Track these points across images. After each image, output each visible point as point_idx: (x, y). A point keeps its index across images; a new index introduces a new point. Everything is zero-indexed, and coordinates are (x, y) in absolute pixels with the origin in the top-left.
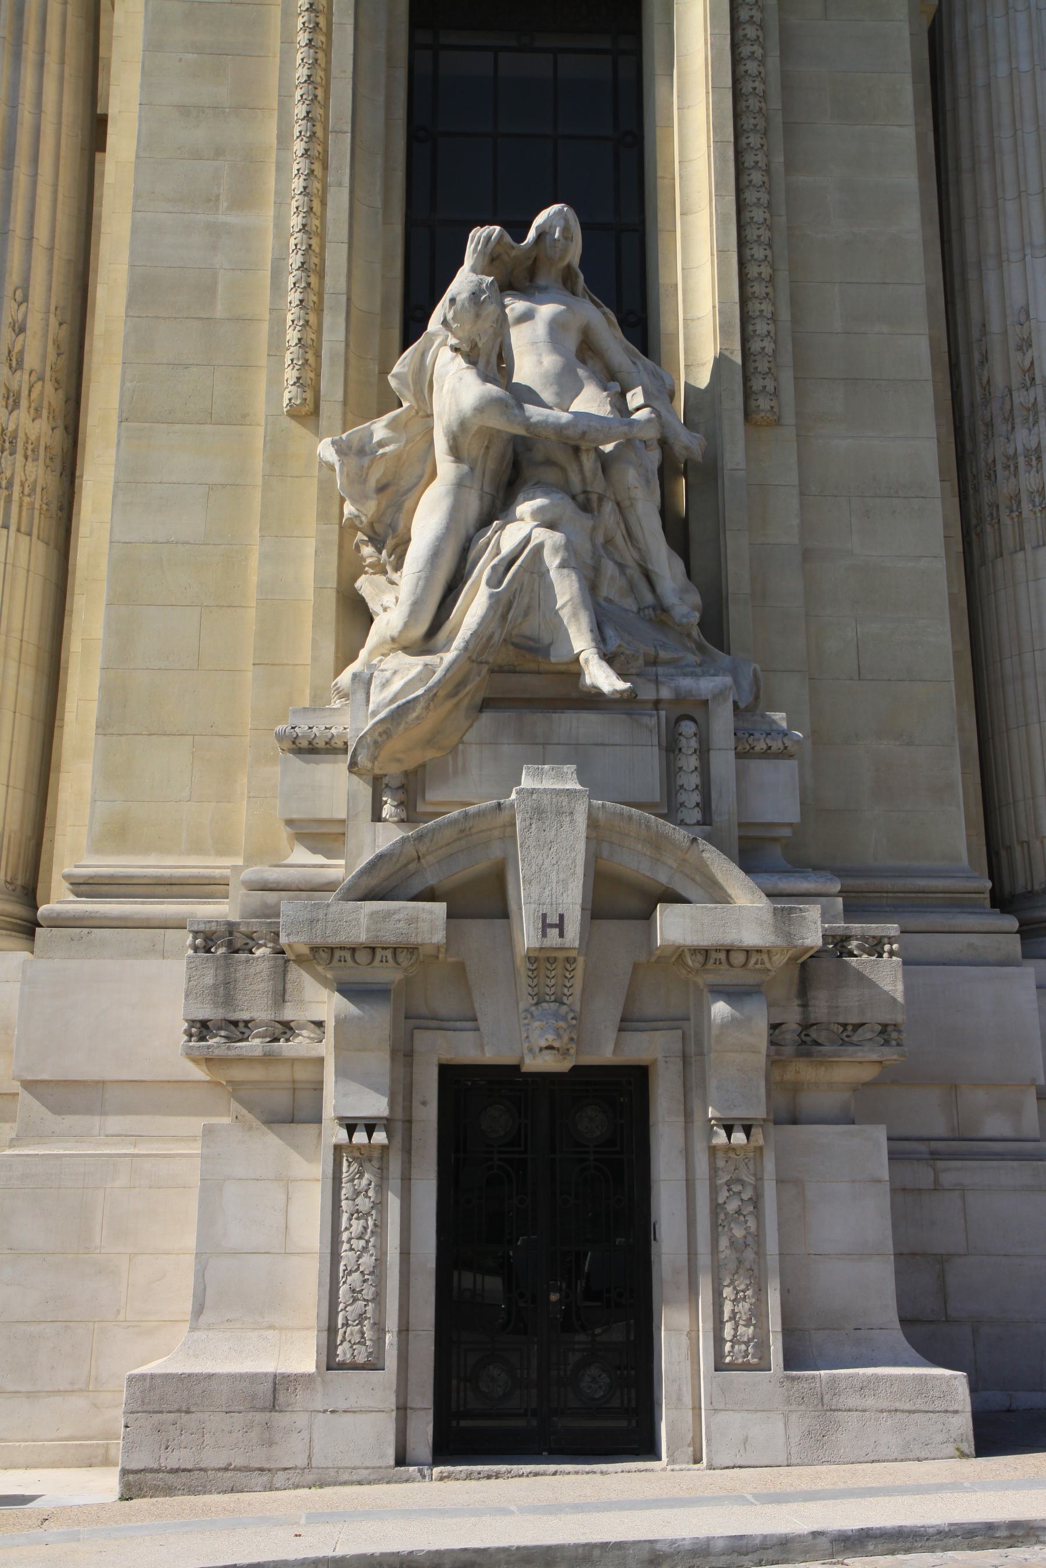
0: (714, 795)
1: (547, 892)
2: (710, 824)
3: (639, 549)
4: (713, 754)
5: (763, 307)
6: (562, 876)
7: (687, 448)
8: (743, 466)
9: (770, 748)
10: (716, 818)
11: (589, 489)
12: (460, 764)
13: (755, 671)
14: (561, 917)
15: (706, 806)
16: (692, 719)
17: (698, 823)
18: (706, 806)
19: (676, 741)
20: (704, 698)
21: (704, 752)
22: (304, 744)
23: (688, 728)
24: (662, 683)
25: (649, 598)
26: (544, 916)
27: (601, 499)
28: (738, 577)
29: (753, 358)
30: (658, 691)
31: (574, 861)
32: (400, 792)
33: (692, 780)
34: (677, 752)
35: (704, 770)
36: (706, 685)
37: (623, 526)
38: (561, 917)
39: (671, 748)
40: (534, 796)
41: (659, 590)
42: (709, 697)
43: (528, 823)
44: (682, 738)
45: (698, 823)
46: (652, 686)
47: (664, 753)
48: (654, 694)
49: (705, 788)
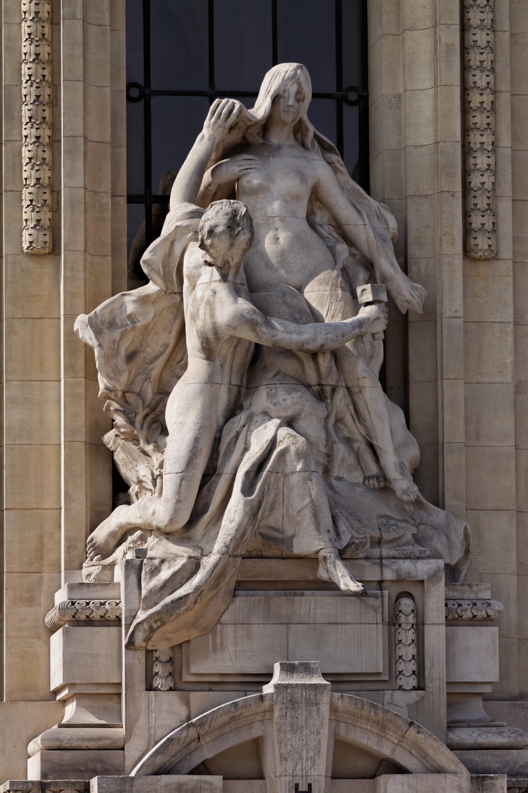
0: (427, 664)
1: (299, 767)
2: (423, 689)
3: (366, 427)
4: (426, 627)
5: (484, 139)
6: (311, 754)
7: (408, 302)
8: (461, 314)
9: (475, 616)
10: (428, 684)
11: (324, 383)
12: (218, 642)
13: (466, 528)
14: (310, 786)
15: (420, 673)
16: (409, 595)
17: (414, 689)
18: (420, 673)
19: (397, 617)
20: (421, 579)
21: (419, 627)
22: (83, 617)
23: (406, 604)
24: (385, 565)
25: (373, 469)
26: (297, 785)
27: (334, 390)
28: (453, 428)
29: (473, 193)
30: (382, 572)
31: (319, 741)
32: (169, 665)
33: (408, 651)
34: (397, 627)
35: (419, 642)
36: (422, 568)
37: (351, 407)
38: (310, 786)
39: (393, 622)
40: (289, 691)
41: (382, 463)
42: (425, 578)
43: (284, 712)
44: (401, 614)
45: (414, 689)
46: (377, 568)
47: (386, 628)
48: (379, 575)
49: (420, 658)
